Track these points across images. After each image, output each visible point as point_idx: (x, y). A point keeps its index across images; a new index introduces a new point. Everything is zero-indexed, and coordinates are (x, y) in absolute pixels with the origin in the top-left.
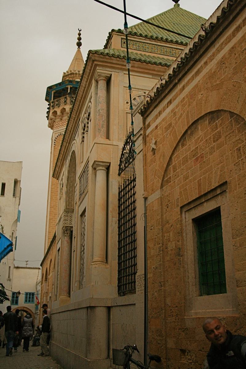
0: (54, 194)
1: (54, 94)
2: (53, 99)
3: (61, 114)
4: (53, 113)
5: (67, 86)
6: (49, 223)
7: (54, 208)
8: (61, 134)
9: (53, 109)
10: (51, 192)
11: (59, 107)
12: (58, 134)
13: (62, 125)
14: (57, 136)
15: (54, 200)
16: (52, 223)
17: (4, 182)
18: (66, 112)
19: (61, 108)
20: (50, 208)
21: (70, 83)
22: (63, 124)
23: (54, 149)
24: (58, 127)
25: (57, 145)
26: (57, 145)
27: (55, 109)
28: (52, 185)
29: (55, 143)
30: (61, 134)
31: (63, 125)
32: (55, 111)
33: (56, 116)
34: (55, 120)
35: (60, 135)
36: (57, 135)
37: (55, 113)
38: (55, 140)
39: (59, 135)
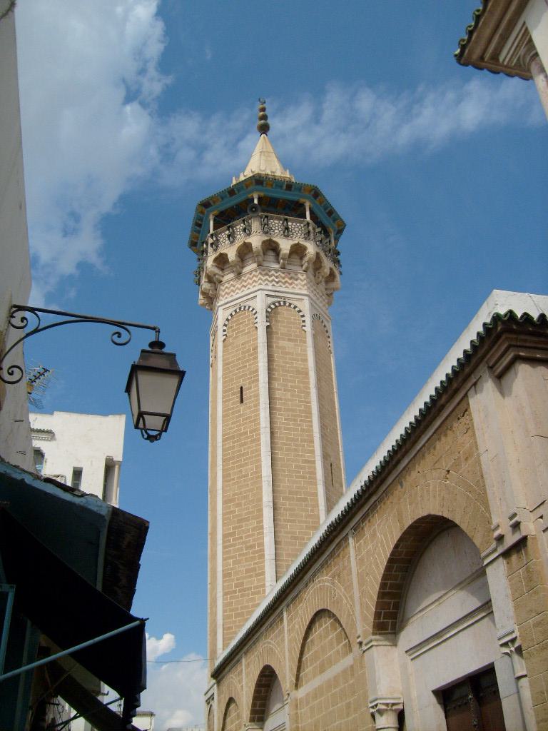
0: (233, 463)
1: (214, 220)
2: (214, 230)
3: (239, 260)
4: (215, 260)
5: (250, 196)
6: (224, 547)
7: (237, 502)
8: (240, 308)
9: (215, 250)
10: (224, 461)
11: (232, 243)
12: (234, 309)
13: (243, 286)
14: (231, 315)
15: (234, 479)
16: (234, 545)
17: (77, 465)
18: (254, 250)
19: (238, 243)
20: (225, 502)
21: (259, 187)
22: (245, 284)
23: (224, 347)
24: (232, 293)
25: (230, 336)
26: (230, 336)
27: (222, 250)
28: (224, 441)
29: (225, 333)
30: (240, 308)
31: (245, 287)
32: (221, 254)
33: (222, 270)
34: (221, 278)
35: (238, 310)
36: (231, 311)
37: (222, 261)
38: (225, 325)
39: (235, 311)
